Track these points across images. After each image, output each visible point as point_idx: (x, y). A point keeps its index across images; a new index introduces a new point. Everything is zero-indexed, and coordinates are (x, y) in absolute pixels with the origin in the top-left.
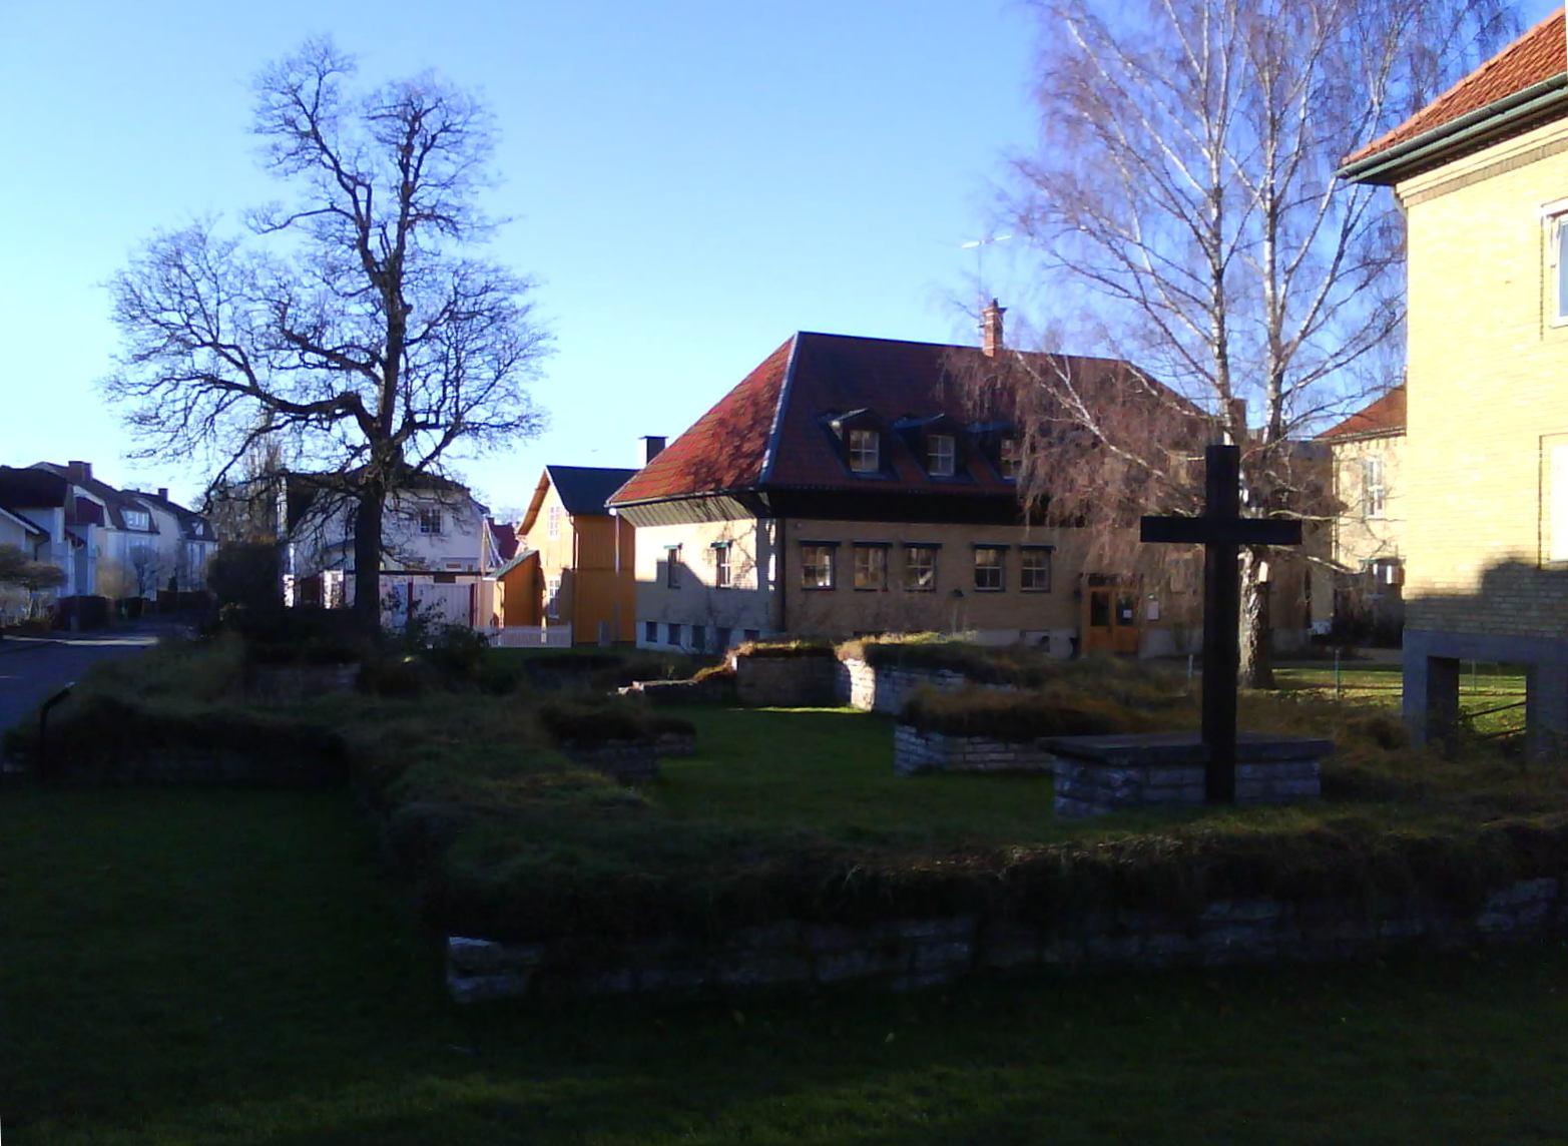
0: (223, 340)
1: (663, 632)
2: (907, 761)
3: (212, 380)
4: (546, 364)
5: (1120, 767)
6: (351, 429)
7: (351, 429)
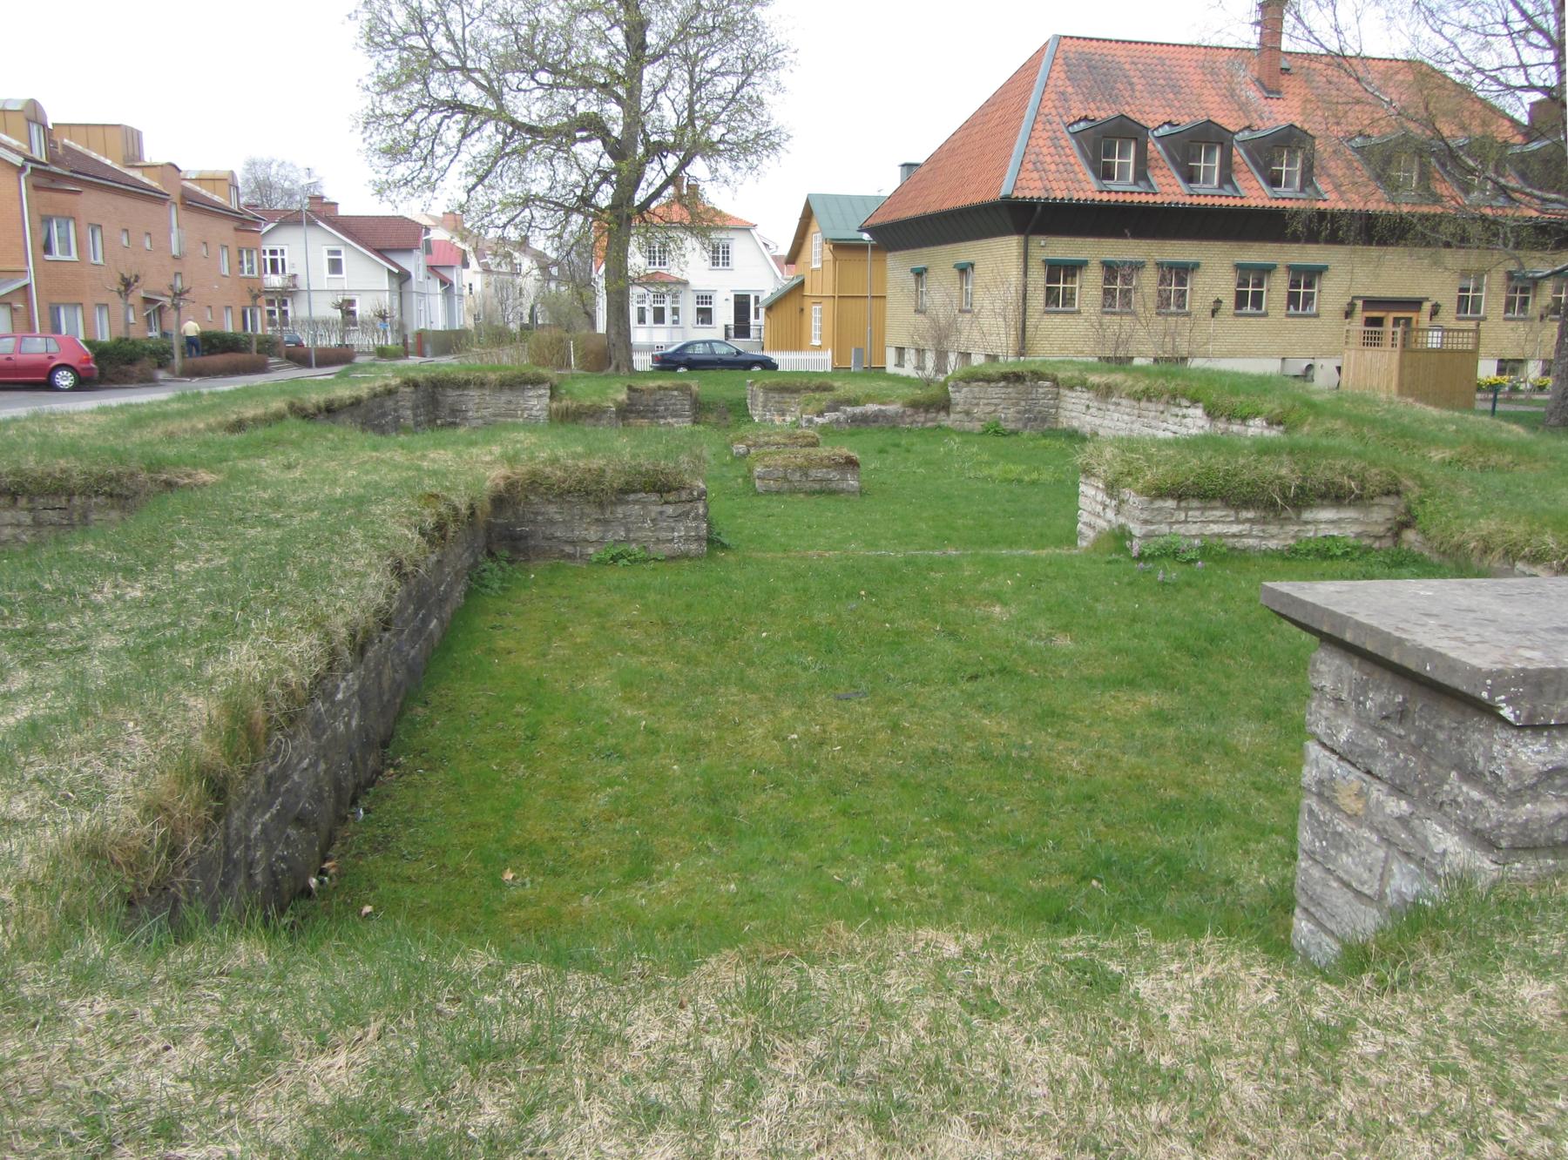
0: (470, 65)
1: (910, 356)
2: (1089, 525)
3: (455, 106)
4: (782, 75)
5: (1532, 727)
6: (591, 152)
7: (591, 152)
